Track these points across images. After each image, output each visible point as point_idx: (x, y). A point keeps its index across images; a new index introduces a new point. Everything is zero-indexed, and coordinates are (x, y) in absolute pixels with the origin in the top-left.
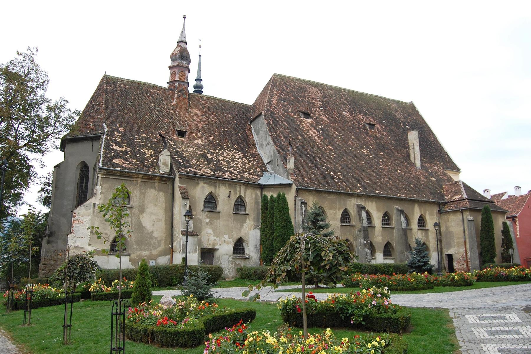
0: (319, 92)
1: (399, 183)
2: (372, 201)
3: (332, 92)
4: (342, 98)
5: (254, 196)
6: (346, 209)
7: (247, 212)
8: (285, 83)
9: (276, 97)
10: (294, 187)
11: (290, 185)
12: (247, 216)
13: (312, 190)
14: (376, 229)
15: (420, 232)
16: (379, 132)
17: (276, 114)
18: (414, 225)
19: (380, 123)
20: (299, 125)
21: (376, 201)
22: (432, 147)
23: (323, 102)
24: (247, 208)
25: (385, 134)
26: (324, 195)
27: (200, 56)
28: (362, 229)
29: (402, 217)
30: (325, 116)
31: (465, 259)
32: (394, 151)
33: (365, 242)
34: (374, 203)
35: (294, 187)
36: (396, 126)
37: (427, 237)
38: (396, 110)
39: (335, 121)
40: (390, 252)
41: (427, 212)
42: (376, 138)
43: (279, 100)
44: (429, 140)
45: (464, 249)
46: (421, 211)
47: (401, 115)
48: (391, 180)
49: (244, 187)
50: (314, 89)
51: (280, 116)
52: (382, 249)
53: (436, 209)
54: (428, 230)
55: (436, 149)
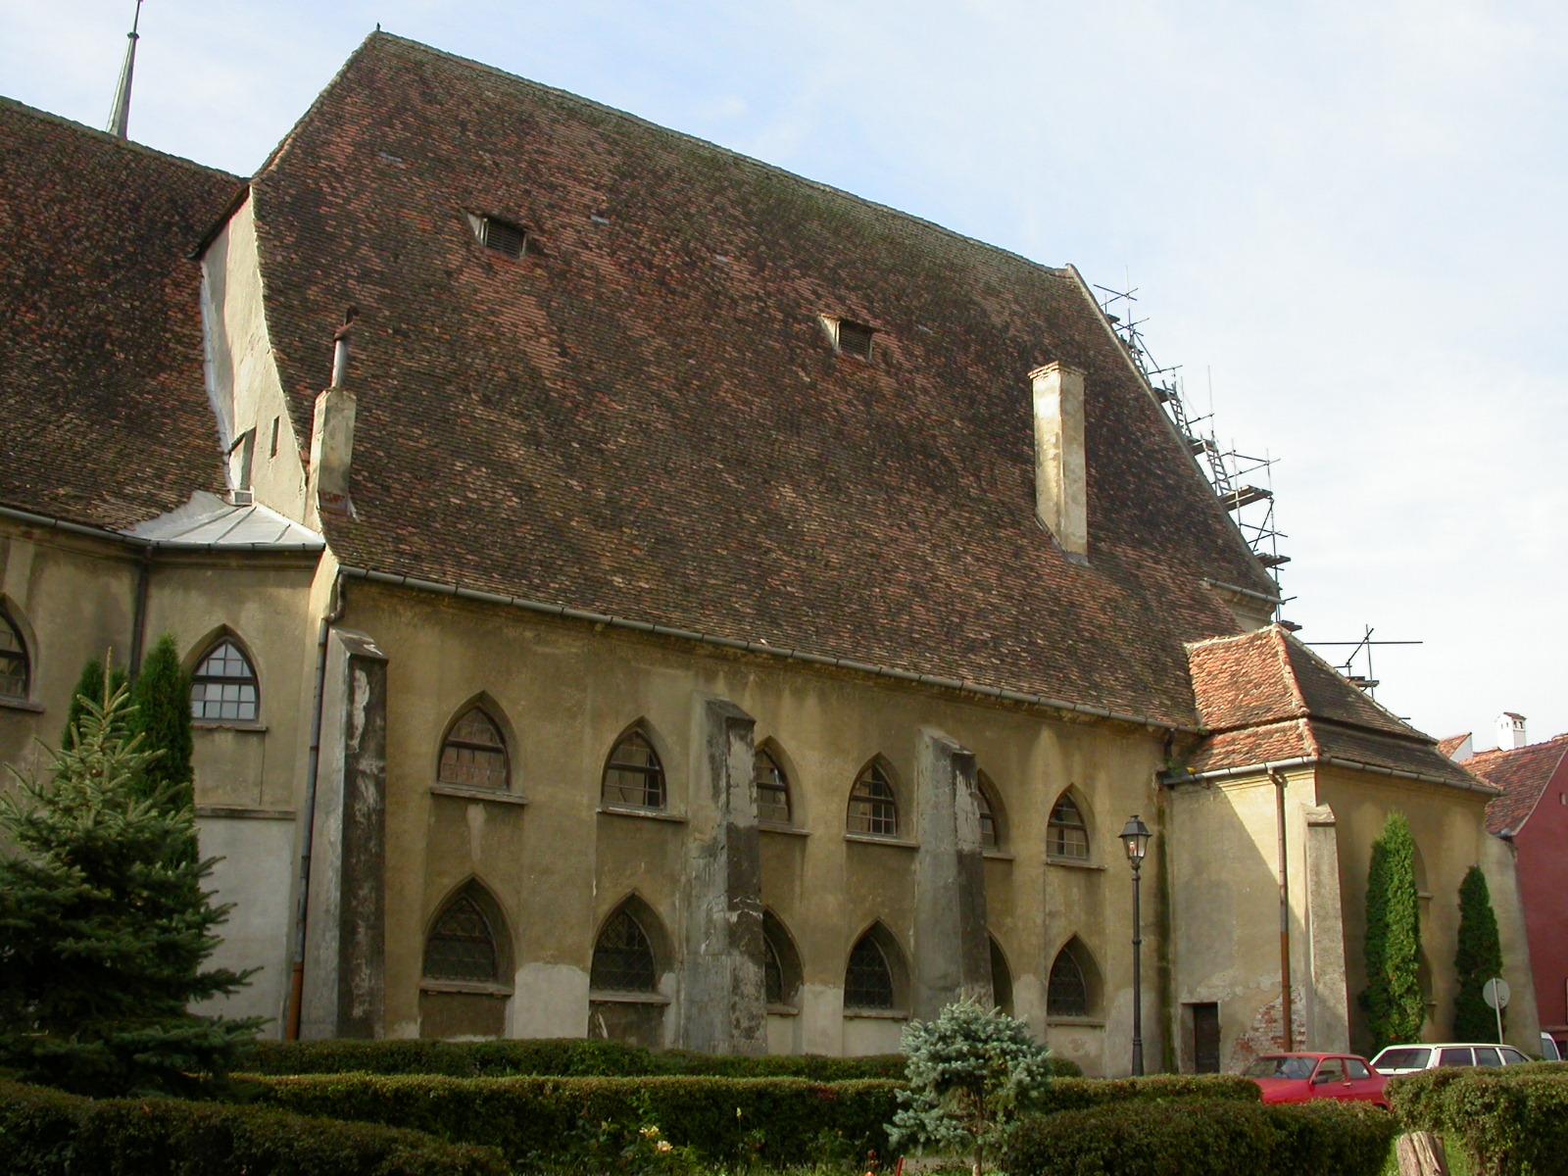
0: (601, 146)
1: (963, 616)
2: (798, 694)
3: (667, 160)
4: (714, 192)
5: (88, 608)
6: (641, 722)
7: (35, 698)
8: (423, 81)
9: (352, 130)
10: (329, 566)
11: (308, 557)
12: (32, 722)
13: (438, 593)
14: (812, 847)
15: (1055, 877)
16: (893, 370)
17: (331, 205)
18: (1030, 838)
19: (904, 331)
20: (449, 274)
21: (823, 697)
22: (1150, 473)
23: (613, 190)
24: (38, 674)
25: (920, 380)
26: (511, 633)
27: (134, 36)
28: (723, 839)
29: (962, 790)
30: (612, 254)
31: (1279, 1029)
32: (958, 466)
33: (734, 918)
34: (811, 703)
35: (329, 566)
36: (980, 358)
37: (1094, 907)
38: (990, 291)
39: (663, 283)
40: (884, 980)
41: (1102, 781)
42: (870, 395)
43: (368, 148)
44: (1137, 442)
45: (1279, 978)
46: (1068, 770)
47: (1014, 313)
48: (925, 597)
49: (31, 548)
50: (580, 133)
51: (349, 216)
52: (840, 964)
53: (1144, 766)
54: (1100, 871)
55: (1167, 487)
